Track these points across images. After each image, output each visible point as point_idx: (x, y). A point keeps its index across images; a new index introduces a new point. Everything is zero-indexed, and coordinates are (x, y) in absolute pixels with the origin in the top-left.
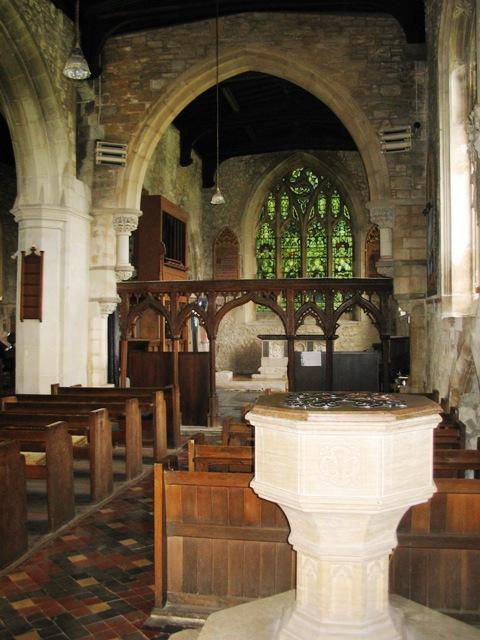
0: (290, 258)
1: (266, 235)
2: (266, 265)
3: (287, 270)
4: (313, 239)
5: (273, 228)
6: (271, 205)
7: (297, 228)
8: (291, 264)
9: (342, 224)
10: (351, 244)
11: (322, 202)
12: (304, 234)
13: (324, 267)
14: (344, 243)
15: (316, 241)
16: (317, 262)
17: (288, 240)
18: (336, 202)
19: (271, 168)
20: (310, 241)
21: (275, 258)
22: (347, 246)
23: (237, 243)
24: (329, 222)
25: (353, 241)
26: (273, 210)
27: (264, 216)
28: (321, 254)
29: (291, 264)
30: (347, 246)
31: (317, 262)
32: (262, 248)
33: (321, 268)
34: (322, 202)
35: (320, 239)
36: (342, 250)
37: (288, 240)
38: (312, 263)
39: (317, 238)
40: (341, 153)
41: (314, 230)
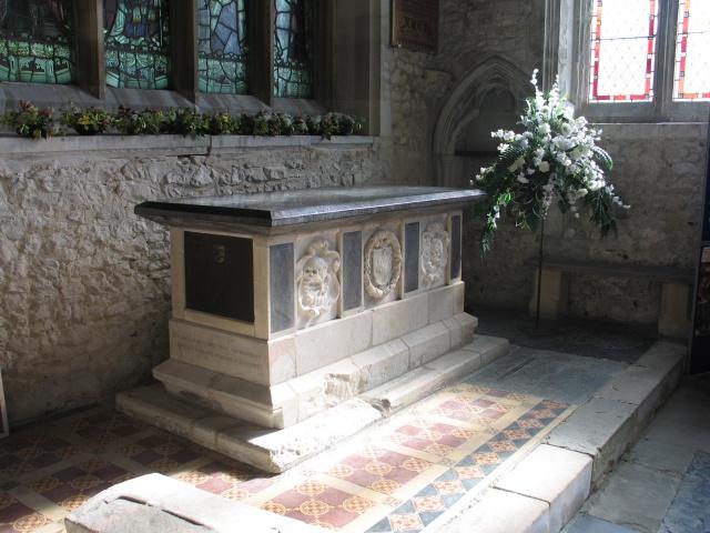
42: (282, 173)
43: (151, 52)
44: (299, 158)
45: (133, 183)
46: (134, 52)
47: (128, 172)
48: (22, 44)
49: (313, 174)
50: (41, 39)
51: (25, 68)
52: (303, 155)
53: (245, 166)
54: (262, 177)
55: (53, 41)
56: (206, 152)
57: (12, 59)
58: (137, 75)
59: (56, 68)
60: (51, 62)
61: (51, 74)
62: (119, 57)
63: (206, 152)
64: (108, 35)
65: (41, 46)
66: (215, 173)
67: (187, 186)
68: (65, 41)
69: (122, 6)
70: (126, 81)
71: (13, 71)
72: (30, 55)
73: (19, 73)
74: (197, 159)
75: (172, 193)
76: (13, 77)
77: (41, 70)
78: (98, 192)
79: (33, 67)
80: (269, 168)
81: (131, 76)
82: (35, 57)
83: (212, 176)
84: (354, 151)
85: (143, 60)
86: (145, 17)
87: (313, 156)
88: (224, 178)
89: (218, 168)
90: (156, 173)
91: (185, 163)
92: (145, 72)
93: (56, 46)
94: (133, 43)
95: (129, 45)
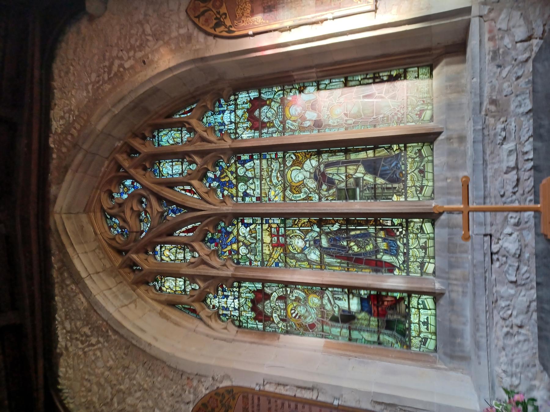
0: (284, 246)
1: (231, 303)
2: (301, 310)
3: (314, 256)
4: (242, 187)
5: (220, 284)
6: (171, 284)
7: (216, 226)
8: (299, 243)
9: (210, 119)
10: (254, 94)
11: (170, 169)
12: (228, 208)
13: (309, 156)
14: (250, 111)
15: (245, 180)
16: (296, 175)
17: (243, 250)
18: (168, 138)
19: (78, 280)
20: (246, 194)
21: (286, 284)
22: (257, 103)
23: (230, 391)
24: (213, 157)
25: (247, 88)
26: (180, 282)
27: (189, 307)
28: (275, 165)
29: (299, 243)
30: (257, 103)
31: (296, 175)
32: (261, 316)
33: (311, 164)
34: (170, 169)
35: (241, 171)
36: (265, 114)
37: (243, 250)
38: (297, 188)
39: (239, 179)
40: (56, 125)
41: (222, 185)
42: (511, 151)
43: (407, 235)
44: (495, 125)
45: (515, 313)
46: (408, 250)
47: (505, 316)
48: (413, 326)
49: (512, 107)
50: (407, 316)
51: (427, 329)
52: (492, 121)
53: (502, 196)
54: (513, 176)
55: (408, 307)
56: (488, 237)
57: (422, 335)
58: (424, 248)
59: (425, 308)
60: (422, 311)
61: (429, 312)
62: (413, 262)
63: (488, 238)
64: (399, 269)
65: (412, 316)
66: (508, 230)
67: (520, 261)
68: (407, 299)
69: (379, 256)
70: (430, 258)
71: (430, 336)
72: (419, 324)
73: (431, 333)
74: (495, 248)
75: (525, 277)
76: (434, 337)
77: (427, 318)
78: (521, 343)
79: (426, 323)
80: (505, 169)
81: (425, 253)
82: (419, 321)
83: (510, 235)
84: (488, 46)
85: (413, 243)
86: (384, 240)
87: (493, 108)
88: (513, 221)
89: (503, 227)
90: (508, 290)
91: (498, 260)
92: (422, 241)
93: (411, 306)
94: (402, 250)
95: (405, 254)
